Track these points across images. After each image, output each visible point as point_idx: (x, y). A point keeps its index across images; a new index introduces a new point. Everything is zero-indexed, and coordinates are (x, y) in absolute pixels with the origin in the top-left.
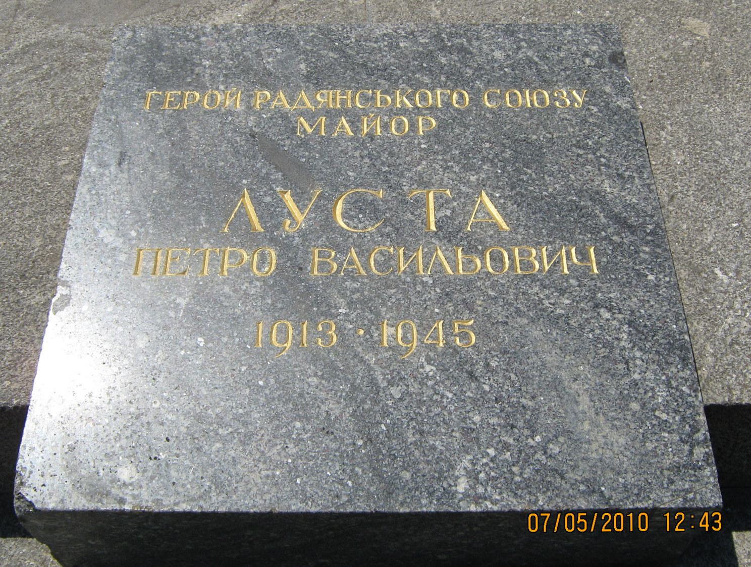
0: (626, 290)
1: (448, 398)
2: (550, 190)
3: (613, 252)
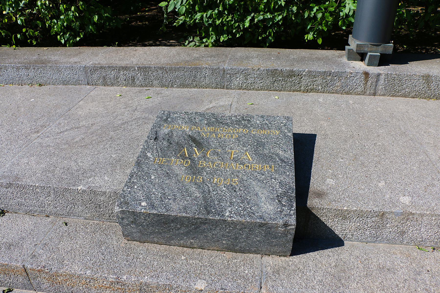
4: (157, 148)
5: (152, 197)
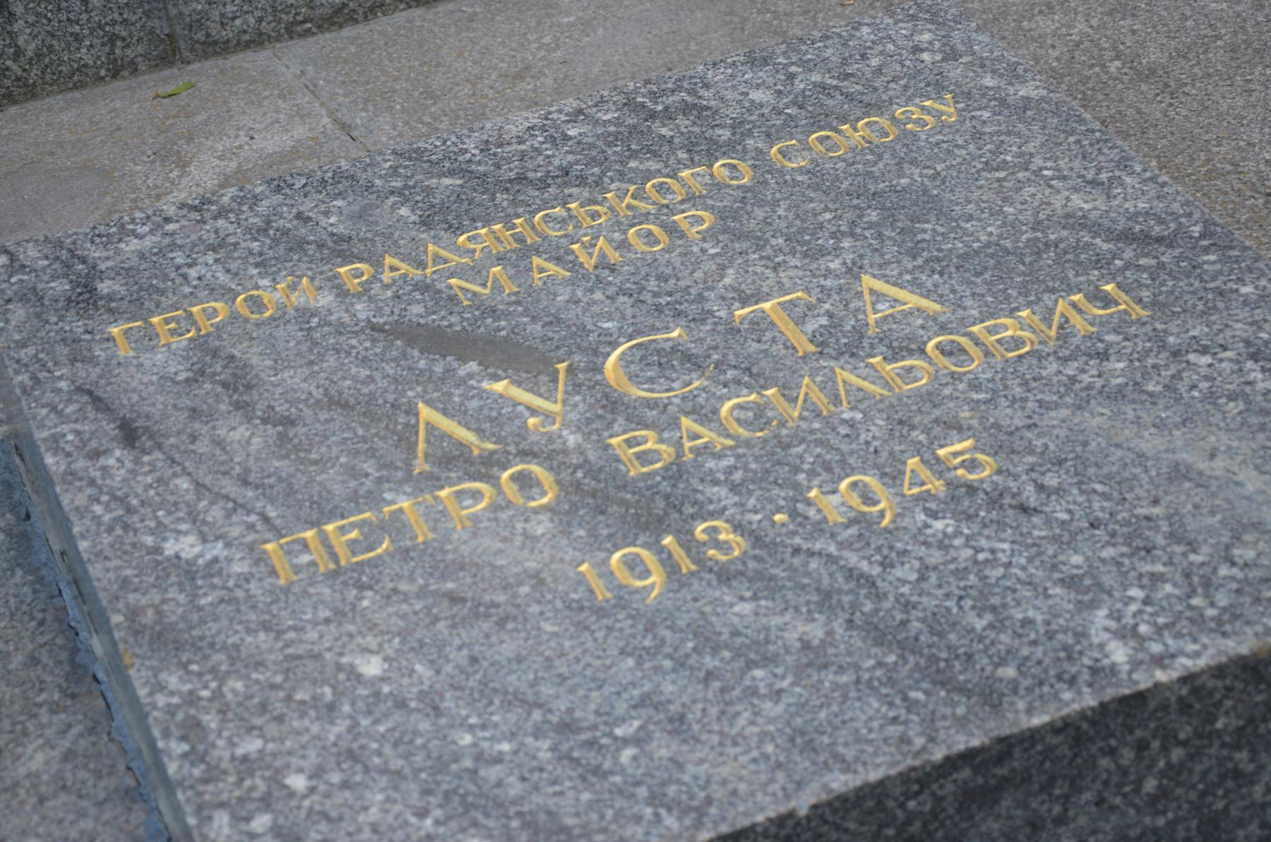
0: (1213, 318)
1: (1004, 551)
3: (1153, 279)
4: (199, 485)
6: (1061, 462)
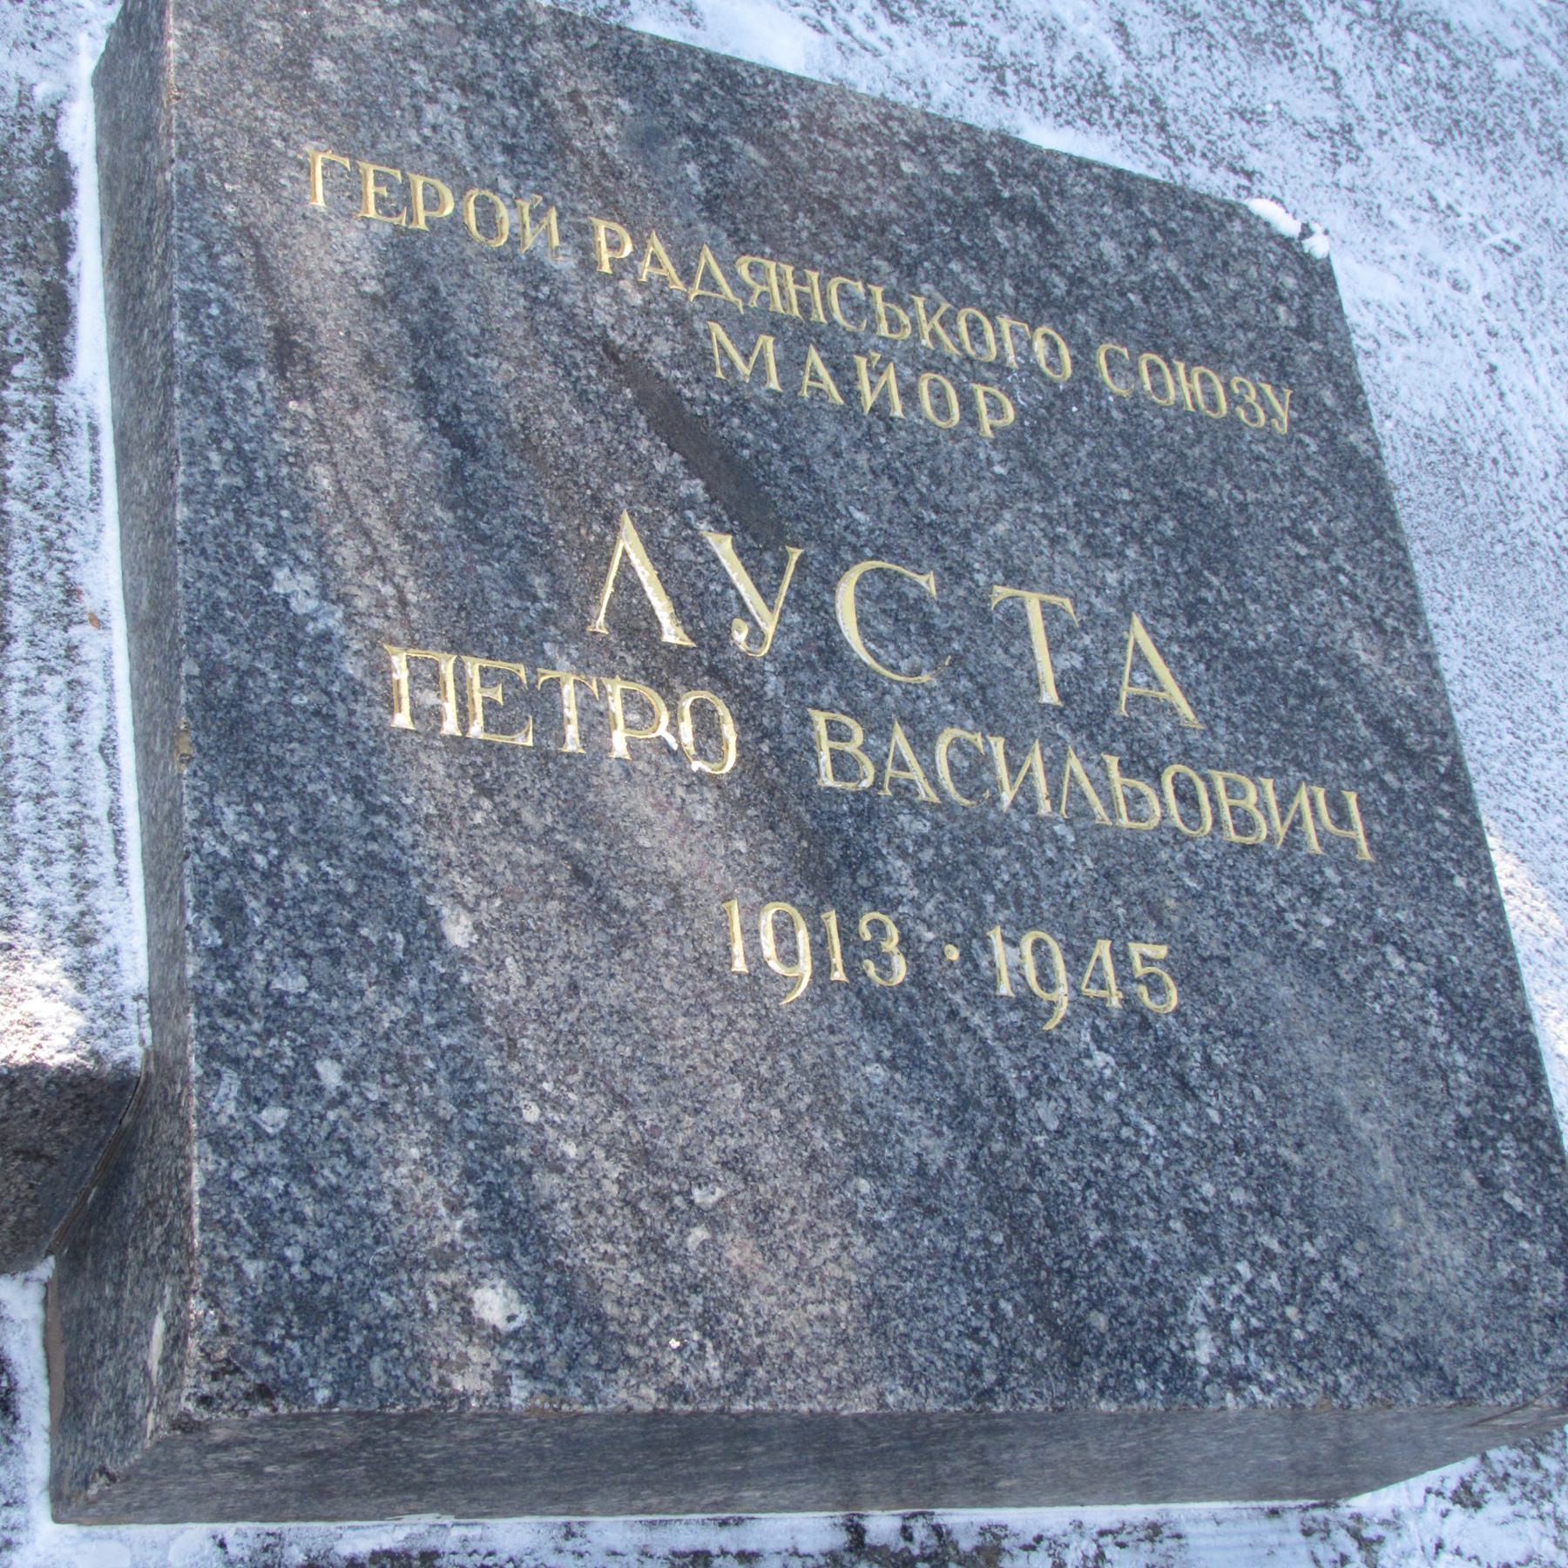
2: (1261, 638)
3: (1390, 811)
5: (548, 1208)
6: (1236, 1033)
